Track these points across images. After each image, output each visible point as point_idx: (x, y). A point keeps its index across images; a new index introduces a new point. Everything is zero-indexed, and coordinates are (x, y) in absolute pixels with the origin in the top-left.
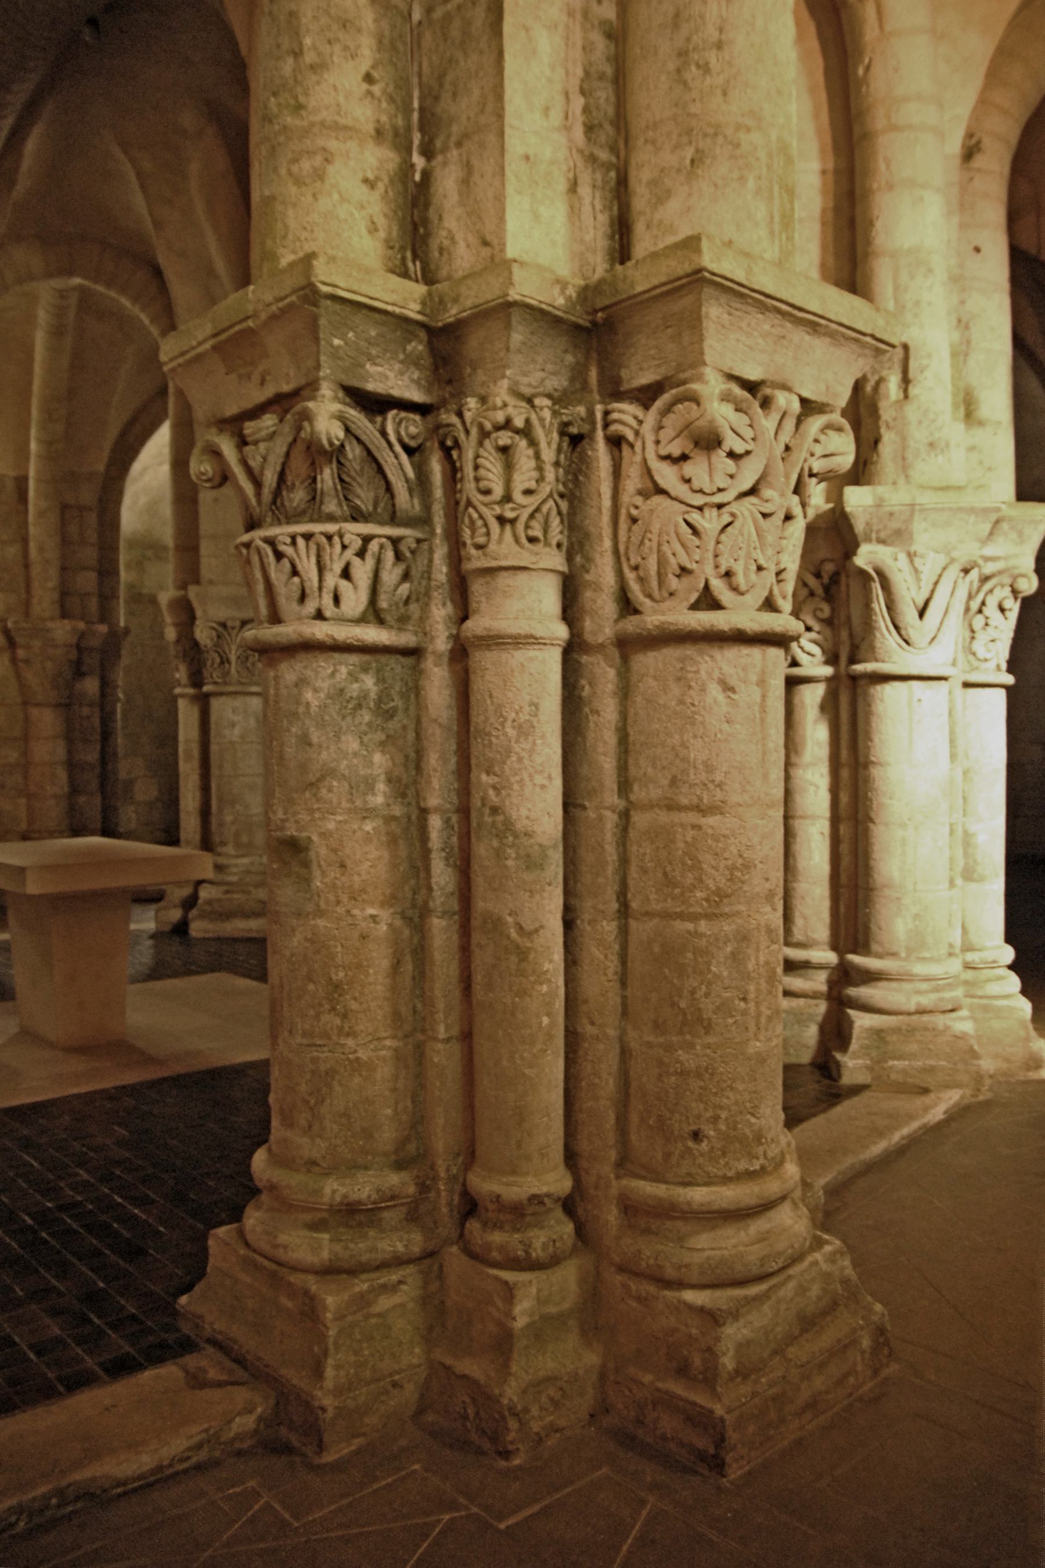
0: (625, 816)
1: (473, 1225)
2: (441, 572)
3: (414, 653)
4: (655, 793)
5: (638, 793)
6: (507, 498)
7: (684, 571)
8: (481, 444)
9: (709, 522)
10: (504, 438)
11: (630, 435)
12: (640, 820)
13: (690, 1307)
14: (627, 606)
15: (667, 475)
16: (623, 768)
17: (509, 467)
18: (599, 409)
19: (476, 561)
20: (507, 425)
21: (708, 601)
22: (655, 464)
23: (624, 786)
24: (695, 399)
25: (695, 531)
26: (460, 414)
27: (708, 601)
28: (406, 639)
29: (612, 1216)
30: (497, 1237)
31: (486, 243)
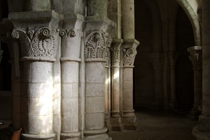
0: (123, 81)
1: (113, 116)
2: (110, 61)
3: (108, 68)
4: (126, 79)
5: (124, 79)
6: (117, 56)
7: (129, 62)
8: (116, 52)
9: (131, 59)
10: (118, 51)
11: (125, 52)
12: (124, 81)
13: (131, 119)
14: (123, 65)
15: (128, 55)
16: (123, 77)
17: (117, 54)
18: (122, 49)
19: (115, 61)
20: (118, 51)
21: (130, 65)
22: (127, 54)
23: (123, 79)
24: (132, 50)
25: (130, 59)
26: (113, 49)
27: (130, 65)
28: (108, 67)
29: (123, 114)
30: (116, 116)
31: (115, 35)
